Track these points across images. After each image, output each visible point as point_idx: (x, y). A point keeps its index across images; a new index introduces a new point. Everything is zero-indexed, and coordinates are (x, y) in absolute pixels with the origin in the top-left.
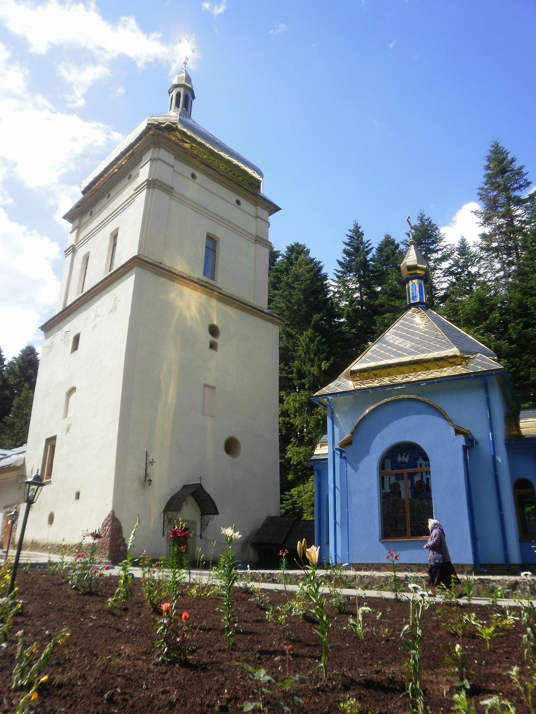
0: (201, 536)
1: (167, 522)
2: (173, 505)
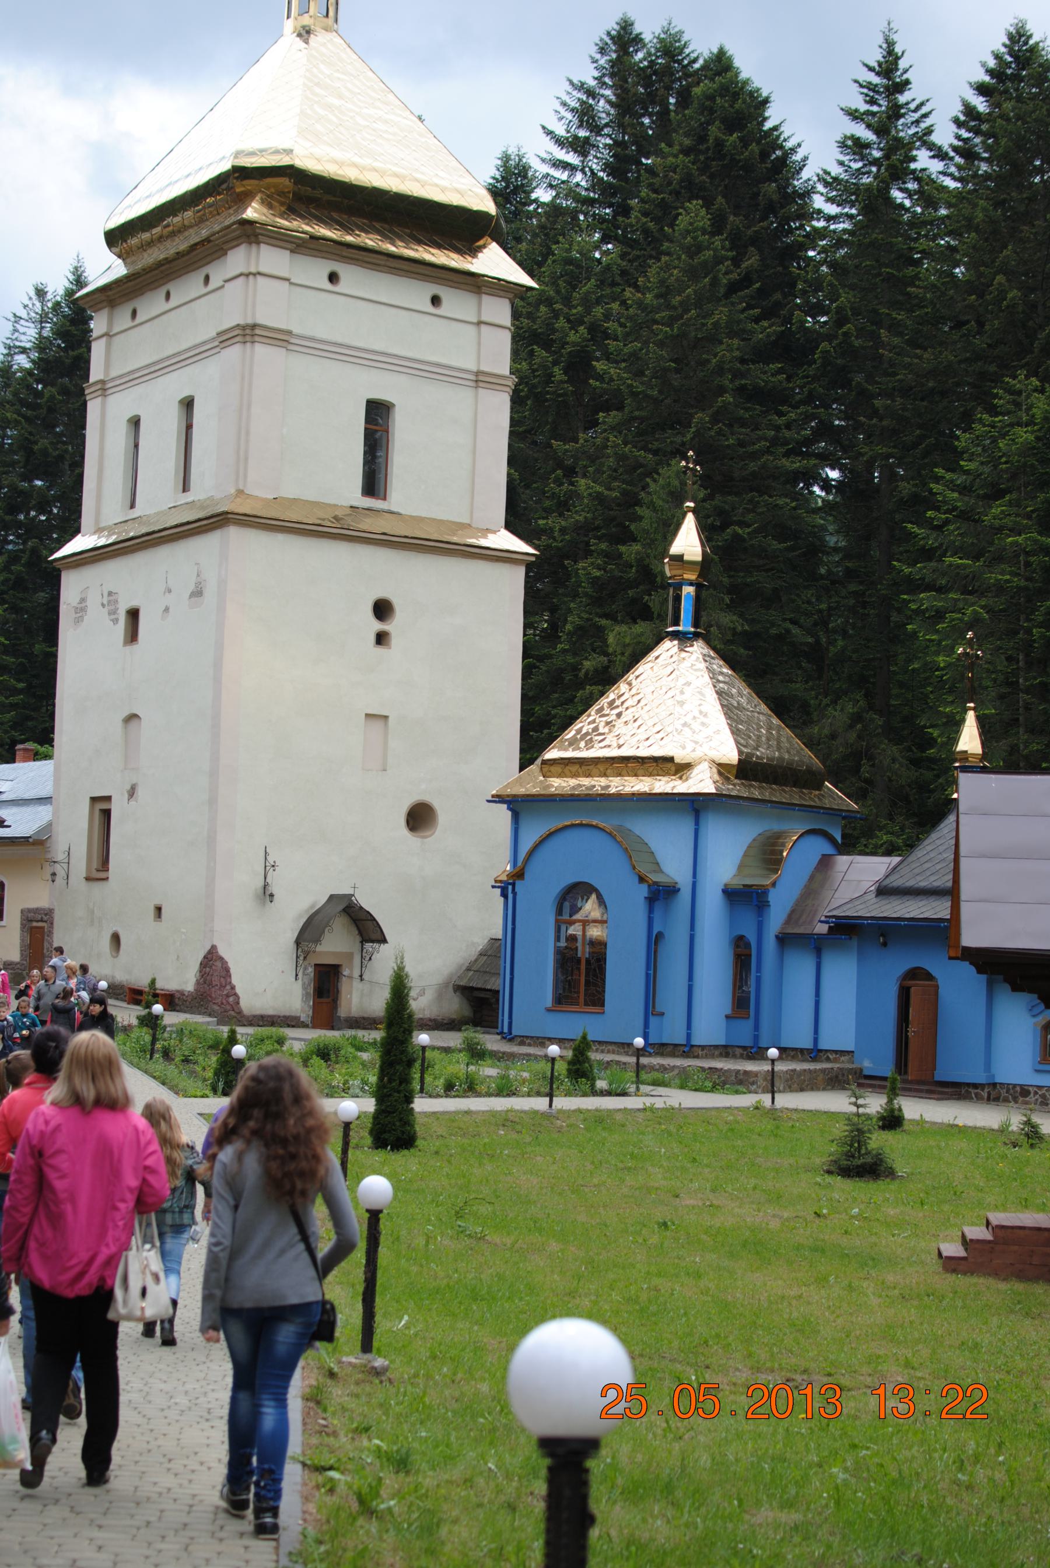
0: (361, 976)
1: (302, 958)
2: (309, 933)
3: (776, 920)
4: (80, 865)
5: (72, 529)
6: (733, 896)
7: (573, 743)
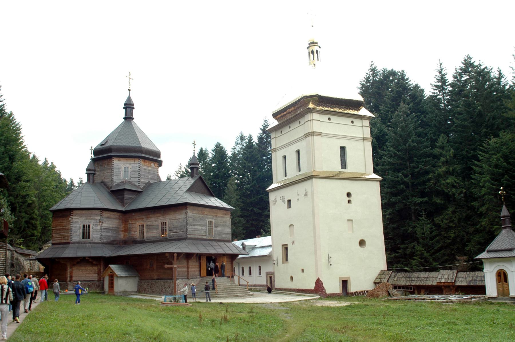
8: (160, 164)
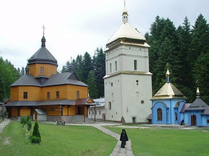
3: (179, 111)
4: (108, 109)
5: (105, 75)
6: (175, 108)
7: (158, 94)
8: (57, 66)
